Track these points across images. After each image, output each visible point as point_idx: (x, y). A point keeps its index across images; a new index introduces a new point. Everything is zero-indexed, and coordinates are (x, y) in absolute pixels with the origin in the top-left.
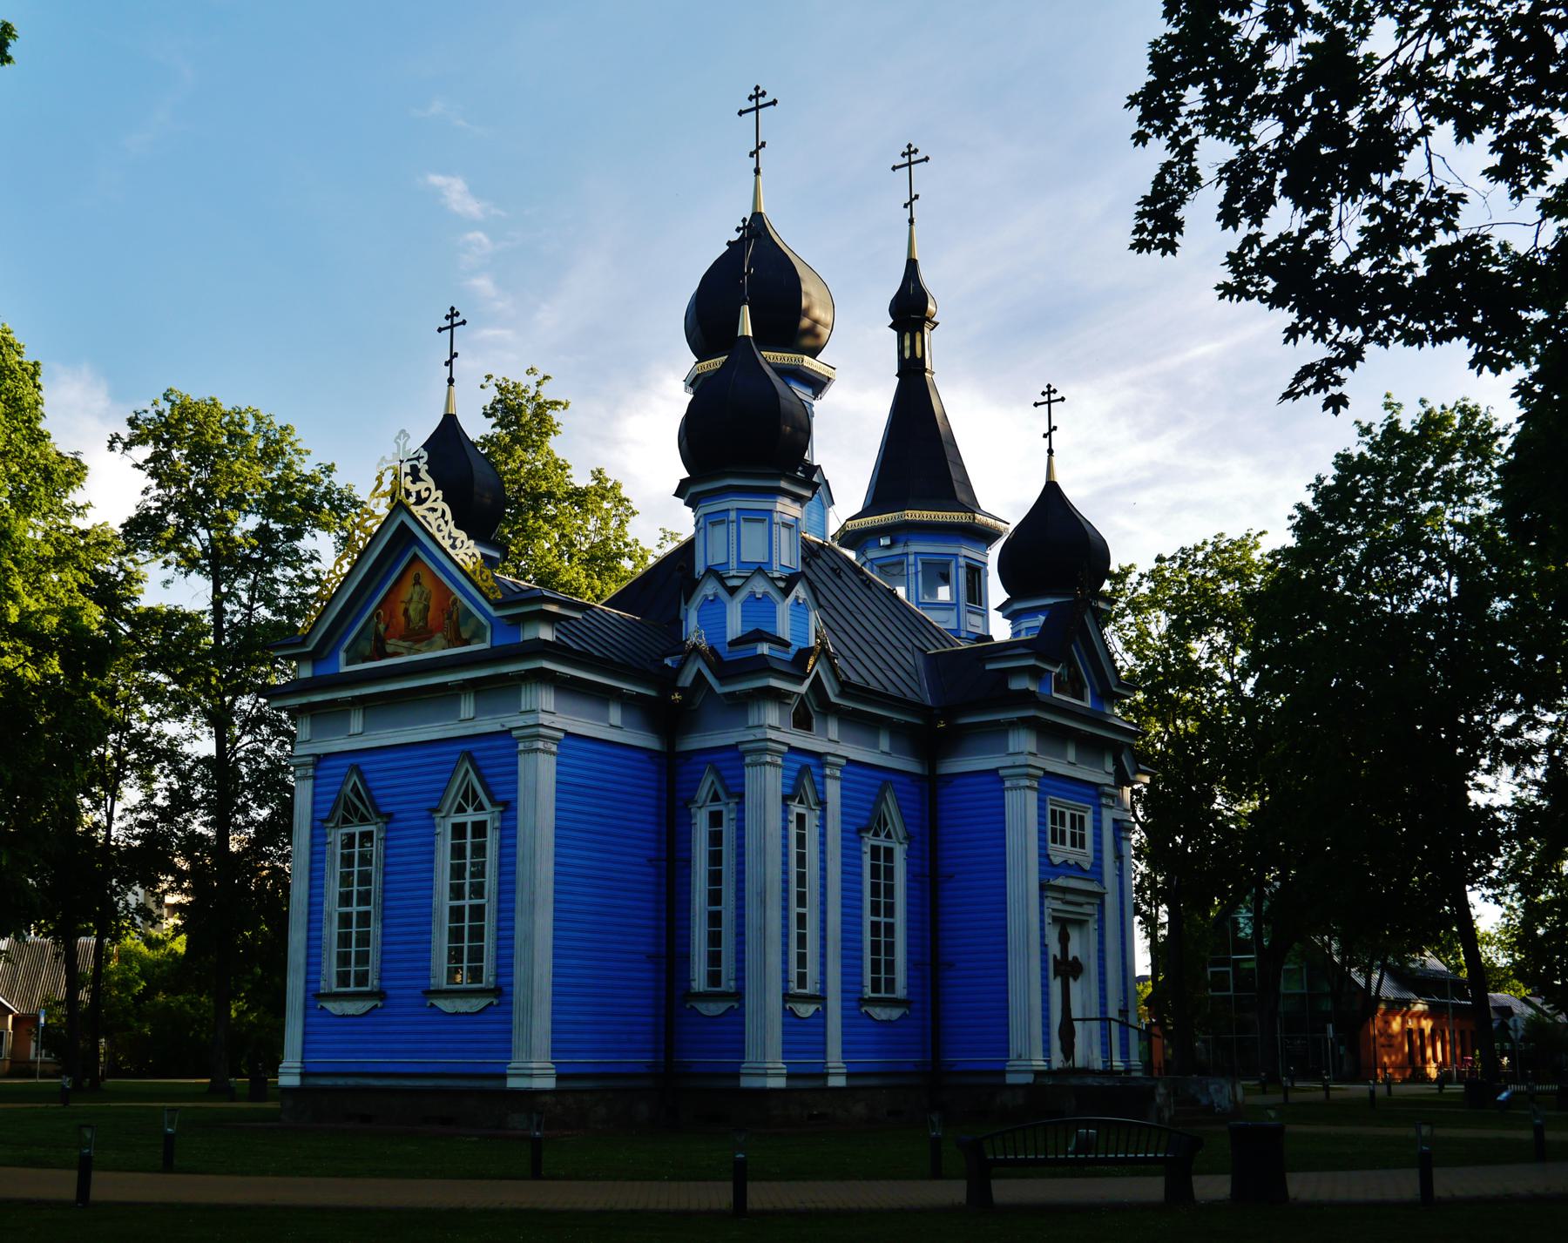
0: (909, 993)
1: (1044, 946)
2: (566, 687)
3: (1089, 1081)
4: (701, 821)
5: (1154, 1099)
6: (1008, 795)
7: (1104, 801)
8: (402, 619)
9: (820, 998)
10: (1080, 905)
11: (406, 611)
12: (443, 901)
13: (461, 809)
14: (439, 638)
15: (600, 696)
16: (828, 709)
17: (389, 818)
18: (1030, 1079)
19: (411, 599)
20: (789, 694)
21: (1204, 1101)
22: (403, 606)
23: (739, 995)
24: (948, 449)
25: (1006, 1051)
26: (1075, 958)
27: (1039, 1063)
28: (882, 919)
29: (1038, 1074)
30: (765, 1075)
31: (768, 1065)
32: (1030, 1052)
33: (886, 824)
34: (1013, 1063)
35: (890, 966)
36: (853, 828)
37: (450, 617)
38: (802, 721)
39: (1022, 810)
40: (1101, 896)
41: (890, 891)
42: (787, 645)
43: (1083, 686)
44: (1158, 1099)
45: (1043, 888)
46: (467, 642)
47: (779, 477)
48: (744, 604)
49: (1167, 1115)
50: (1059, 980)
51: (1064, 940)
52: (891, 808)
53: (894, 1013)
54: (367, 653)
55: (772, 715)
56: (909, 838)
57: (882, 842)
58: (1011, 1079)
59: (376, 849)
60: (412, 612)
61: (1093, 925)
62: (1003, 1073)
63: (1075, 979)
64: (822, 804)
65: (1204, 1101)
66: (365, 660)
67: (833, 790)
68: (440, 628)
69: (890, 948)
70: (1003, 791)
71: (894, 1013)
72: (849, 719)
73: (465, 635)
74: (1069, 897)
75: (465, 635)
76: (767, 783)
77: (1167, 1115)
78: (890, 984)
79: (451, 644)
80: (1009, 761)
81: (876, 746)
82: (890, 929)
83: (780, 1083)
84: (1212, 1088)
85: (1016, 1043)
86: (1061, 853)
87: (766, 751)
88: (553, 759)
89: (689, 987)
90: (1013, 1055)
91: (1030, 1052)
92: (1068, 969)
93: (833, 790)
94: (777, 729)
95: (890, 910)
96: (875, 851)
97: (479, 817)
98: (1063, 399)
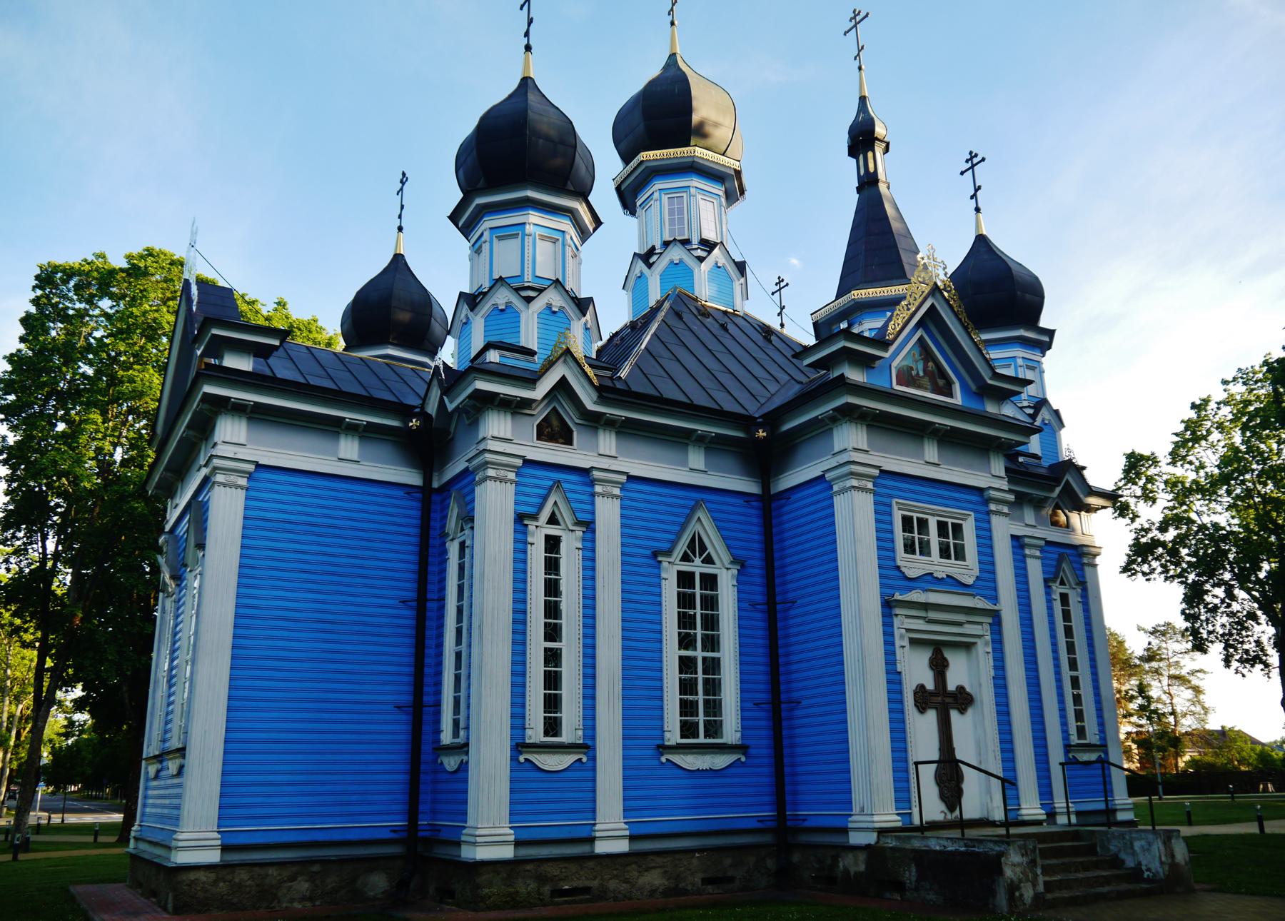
0: (743, 737)
1: (894, 678)
2: (256, 415)
3: (934, 843)
4: (453, 549)
5: (1000, 872)
6: (837, 501)
7: (993, 507)
9: (587, 747)
10: (960, 624)
15: (334, 427)
16: (594, 422)
18: (871, 838)
20: (527, 403)
21: (1130, 863)
23: (464, 748)
24: (901, 244)
25: (849, 803)
26: (961, 689)
27: (888, 816)
28: (699, 654)
29: (882, 832)
30: (474, 844)
31: (490, 832)
32: (874, 807)
33: (703, 548)
34: (856, 820)
35: (714, 707)
36: (648, 552)
38: (554, 431)
39: (855, 517)
40: (996, 616)
41: (711, 622)
42: (531, 353)
43: (949, 383)
44: (1008, 872)
45: (888, 606)
47: (525, 188)
48: (487, 318)
49: (1028, 893)
50: (932, 715)
51: (939, 666)
52: (705, 526)
53: (721, 761)
55: (496, 426)
56: (736, 560)
57: (697, 567)
58: (856, 839)
61: (983, 649)
62: (845, 831)
63: (962, 711)
64: (588, 526)
65: (1130, 863)
67: (608, 513)
69: (713, 687)
70: (831, 498)
71: (721, 761)
72: (626, 430)
74: (933, 615)
76: (495, 502)
77: (1028, 893)
78: (714, 728)
80: (833, 462)
81: (684, 463)
82: (713, 666)
83: (507, 853)
84: (1137, 845)
85: (858, 797)
86: (913, 566)
87: (486, 465)
88: (241, 494)
89: (439, 740)
90: (856, 809)
91: (874, 807)
92: (945, 701)
93: (608, 513)
94: (509, 441)
95: (712, 643)
96: (685, 579)
98: (983, 160)
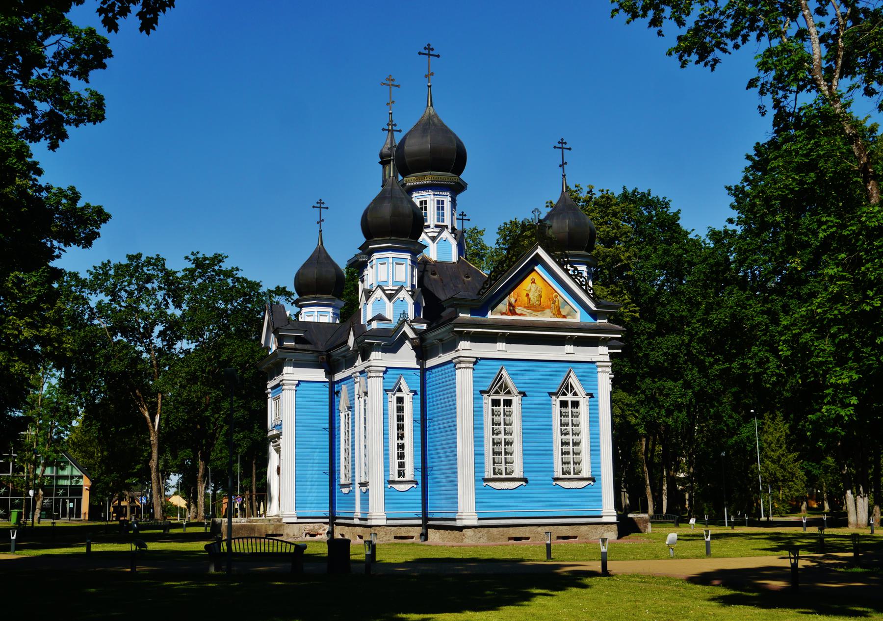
8: (526, 298)
11: (527, 295)
12: (557, 438)
13: (564, 394)
14: (547, 311)
17: (523, 394)
19: (530, 290)
22: (525, 293)
37: (554, 303)
46: (564, 317)
54: (504, 311)
59: (516, 407)
60: (531, 296)
66: (502, 314)
68: (549, 307)
73: (563, 313)
75: (563, 313)
79: (555, 315)
97: (575, 399)
